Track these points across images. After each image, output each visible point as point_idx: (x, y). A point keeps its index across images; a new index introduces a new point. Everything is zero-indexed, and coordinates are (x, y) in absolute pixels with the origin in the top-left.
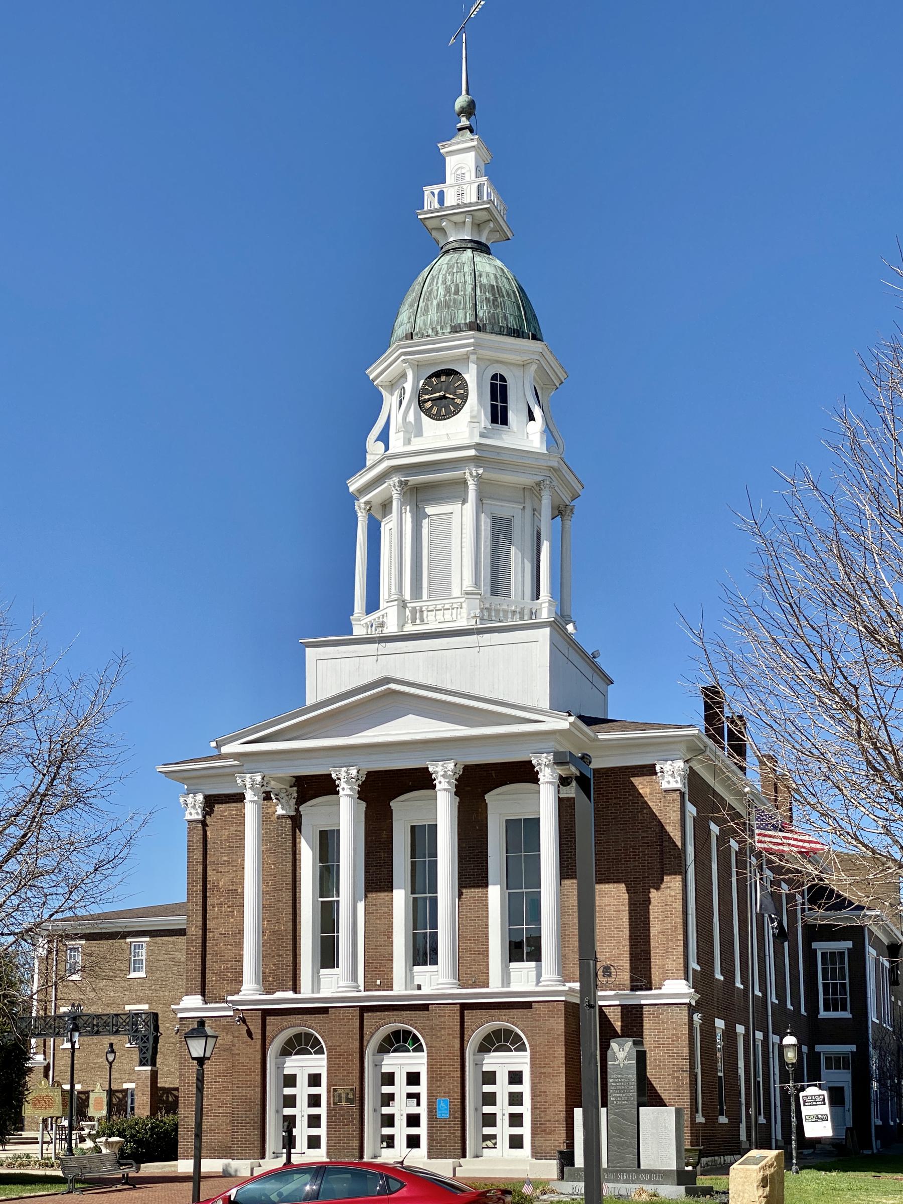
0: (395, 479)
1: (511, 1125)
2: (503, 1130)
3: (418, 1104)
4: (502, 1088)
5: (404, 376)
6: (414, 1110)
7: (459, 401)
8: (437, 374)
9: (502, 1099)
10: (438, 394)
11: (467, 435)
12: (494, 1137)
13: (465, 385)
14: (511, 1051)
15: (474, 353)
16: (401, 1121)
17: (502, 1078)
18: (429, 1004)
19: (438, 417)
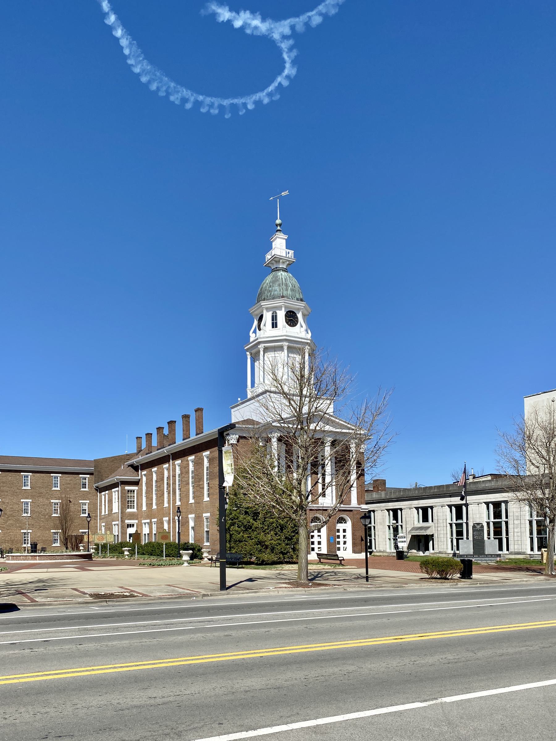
0: (286, 344)
1: (318, 544)
2: (341, 546)
3: (320, 538)
4: (341, 534)
5: (280, 308)
6: (320, 540)
7: (296, 323)
8: (290, 312)
9: (341, 537)
10: (290, 319)
11: (304, 335)
12: (320, 548)
13: (297, 318)
14: (342, 523)
15: (303, 309)
16: (316, 543)
17: (341, 531)
18: (327, 509)
19: (290, 325)
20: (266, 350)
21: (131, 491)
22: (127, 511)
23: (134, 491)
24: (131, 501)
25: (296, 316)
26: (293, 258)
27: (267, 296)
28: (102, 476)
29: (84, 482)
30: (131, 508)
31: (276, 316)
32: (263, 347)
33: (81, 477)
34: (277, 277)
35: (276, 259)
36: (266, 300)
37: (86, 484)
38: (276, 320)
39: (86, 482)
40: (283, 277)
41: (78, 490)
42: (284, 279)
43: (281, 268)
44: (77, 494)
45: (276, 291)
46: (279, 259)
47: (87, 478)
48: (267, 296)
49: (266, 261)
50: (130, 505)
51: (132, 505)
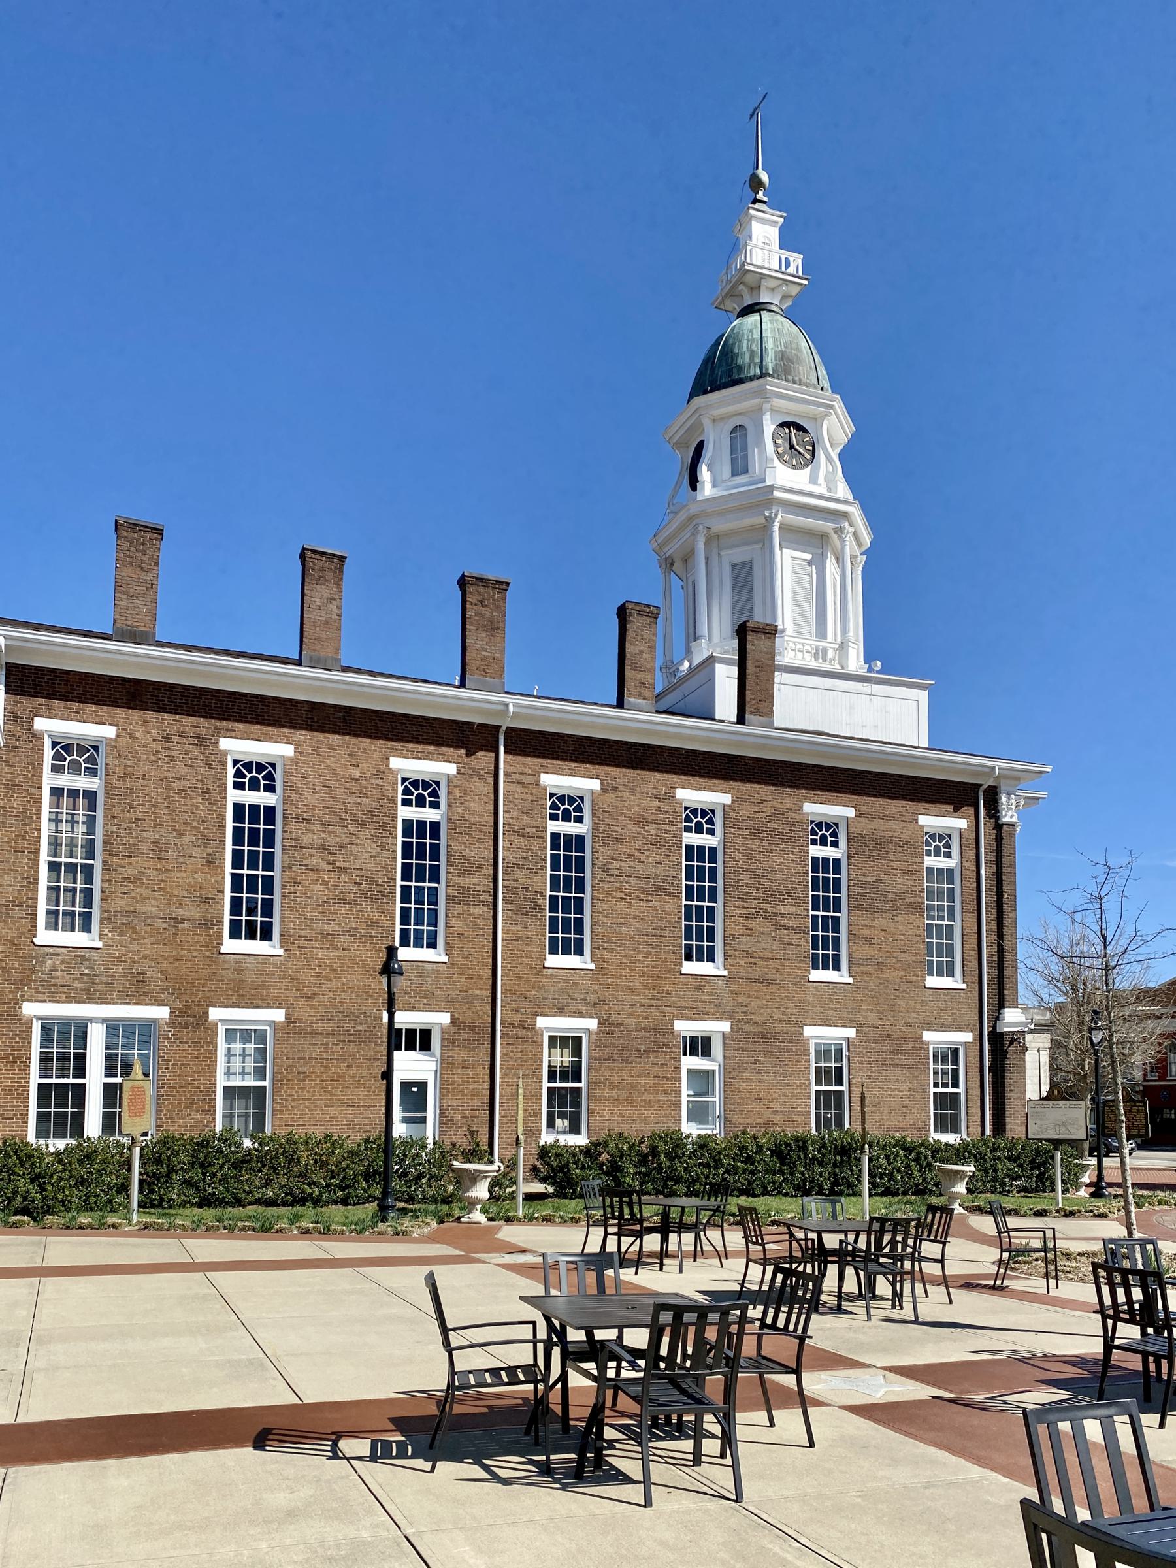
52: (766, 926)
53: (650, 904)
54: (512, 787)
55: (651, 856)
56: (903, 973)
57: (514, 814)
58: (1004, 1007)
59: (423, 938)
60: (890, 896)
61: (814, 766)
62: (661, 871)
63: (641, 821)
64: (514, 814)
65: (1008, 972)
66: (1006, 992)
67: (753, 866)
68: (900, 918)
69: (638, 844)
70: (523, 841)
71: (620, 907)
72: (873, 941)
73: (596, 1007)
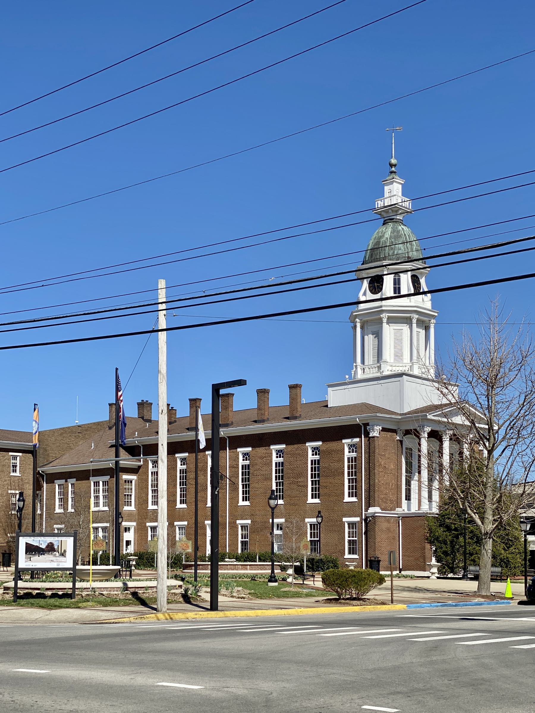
20: (391, 320)
21: (128, 481)
22: (124, 509)
23: (131, 482)
24: (128, 495)
25: (419, 281)
26: (410, 208)
27: (389, 254)
28: (48, 455)
29: (14, 463)
30: (128, 506)
31: (399, 280)
32: (387, 317)
33: (12, 455)
34: (398, 231)
35: (394, 208)
36: (388, 260)
37: (16, 466)
38: (399, 284)
39: (16, 463)
40: (406, 233)
41: (7, 475)
42: (407, 235)
43: (398, 219)
44: (5, 481)
45: (400, 250)
46: (398, 209)
47: (18, 458)
48: (389, 254)
49: (376, 207)
50: (126, 500)
51: (129, 500)
52: (295, 487)
53: (264, 483)
54: (231, 454)
55: (264, 468)
56: (337, 498)
57: (231, 462)
58: (369, 507)
59: (229, 499)
60: (333, 470)
61: (309, 429)
62: (267, 473)
63: (262, 458)
64: (231, 462)
65: (371, 493)
66: (370, 502)
67: (291, 467)
68: (336, 478)
69: (261, 465)
70: (234, 469)
71: (257, 485)
72: (327, 487)
73: (251, 516)
